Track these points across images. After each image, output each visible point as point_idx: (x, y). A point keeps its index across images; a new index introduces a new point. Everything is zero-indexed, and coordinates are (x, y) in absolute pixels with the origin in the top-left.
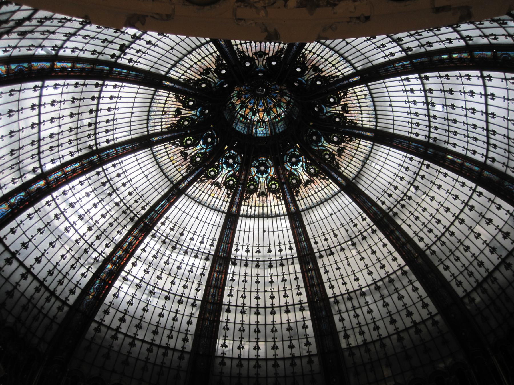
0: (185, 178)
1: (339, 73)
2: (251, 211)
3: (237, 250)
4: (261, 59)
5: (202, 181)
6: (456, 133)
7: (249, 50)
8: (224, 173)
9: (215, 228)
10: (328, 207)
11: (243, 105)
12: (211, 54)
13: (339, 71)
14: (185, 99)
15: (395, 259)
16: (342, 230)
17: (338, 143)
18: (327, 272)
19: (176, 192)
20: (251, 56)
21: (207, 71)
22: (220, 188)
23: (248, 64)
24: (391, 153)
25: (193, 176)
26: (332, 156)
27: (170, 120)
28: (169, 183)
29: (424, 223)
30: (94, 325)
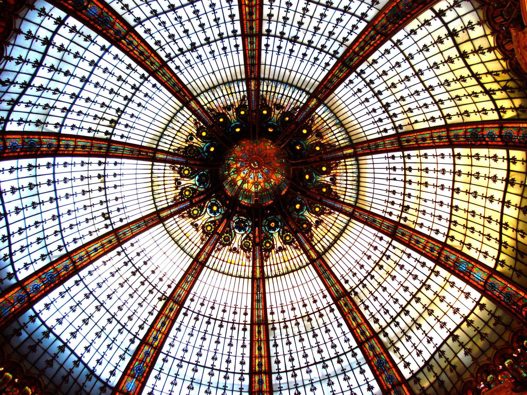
1: (337, 144)
5: (183, 217)
6: (424, 212)
7: (271, 99)
8: (206, 217)
12: (239, 92)
13: (338, 141)
20: (270, 105)
22: (197, 230)
23: (265, 112)
24: (364, 231)
25: (177, 209)
26: (310, 225)
27: (180, 142)
28: (153, 206)
29: (381, 304)
30: (30, 312)
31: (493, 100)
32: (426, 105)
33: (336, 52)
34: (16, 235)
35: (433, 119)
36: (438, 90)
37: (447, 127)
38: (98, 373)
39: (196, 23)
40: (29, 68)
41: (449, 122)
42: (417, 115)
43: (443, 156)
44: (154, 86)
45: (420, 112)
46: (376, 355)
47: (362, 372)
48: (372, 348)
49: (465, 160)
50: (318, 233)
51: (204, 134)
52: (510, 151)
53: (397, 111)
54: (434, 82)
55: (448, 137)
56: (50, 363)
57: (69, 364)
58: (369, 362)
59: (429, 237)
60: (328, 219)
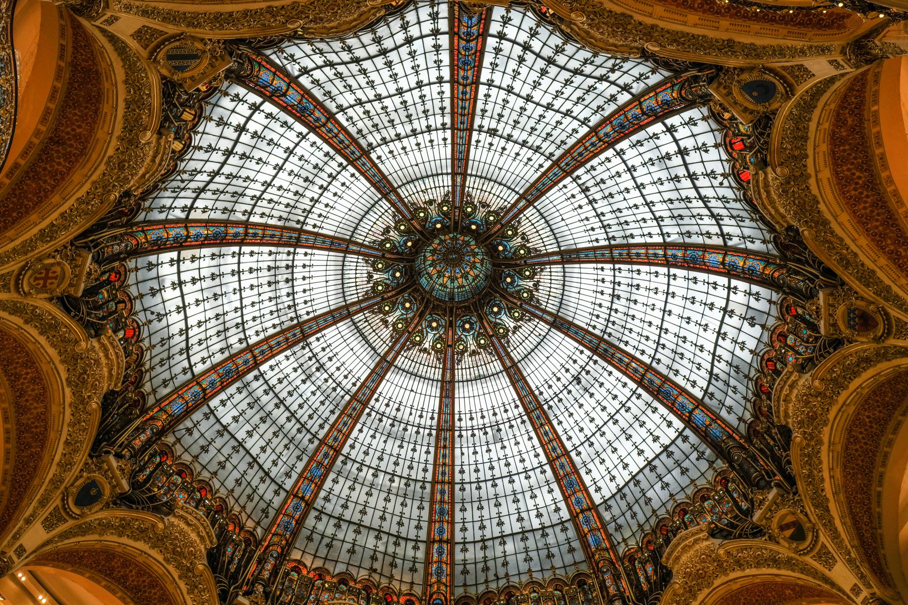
0: (362, 245)
2: (361, 325)
3: (318, 339)
4: (519, 240)
5: (367, 262)
9: (326, 304)
10: (416, 383)
11: (434, 252)
14: (448, 201)
15: (425, 470)
16: (408, 410)
17: (479, 346)
18: (361, 431)
19: (340, 245)
21: (484, 205)
22: (368, 282)
31: (709, 382)
32: (647, 338)
33: (614, 238)
34: (223, 177)
35: (643, 352)
36: (670, 336)
37: (649, 368)
38: (191, 353)
39: (532, 123)
40: (373, 49)
41: (654, 365)
42: (633, 339)
43: (625, 385)
44: (445, 139)
45: (638, 338)
46: (442, 502)
47: (421, 508)
48: (442, 492)
49: (640, 403)
50: (467, 360)
51: (445, 208)
52: (687, 430)
53: (617, 321)
54: (673, 329)
55: (643, 376)
56: (160, 317)
57: (174, 330)
58: (432, 502)
59: (559, 437)
60: (484, 356)
